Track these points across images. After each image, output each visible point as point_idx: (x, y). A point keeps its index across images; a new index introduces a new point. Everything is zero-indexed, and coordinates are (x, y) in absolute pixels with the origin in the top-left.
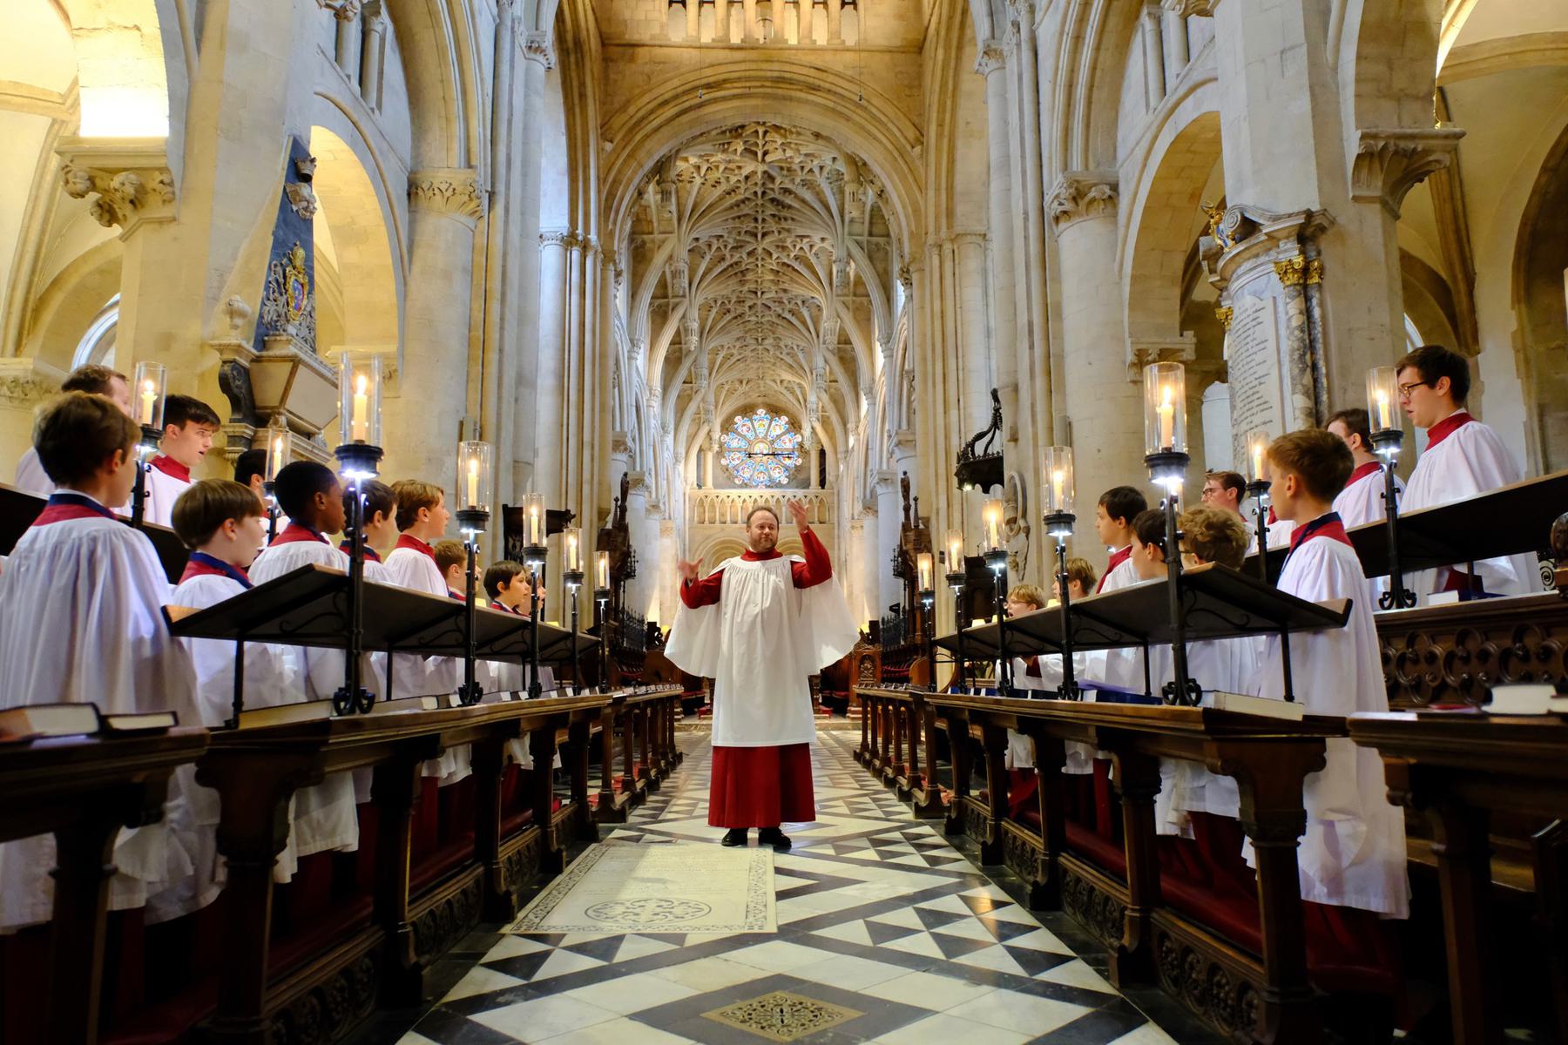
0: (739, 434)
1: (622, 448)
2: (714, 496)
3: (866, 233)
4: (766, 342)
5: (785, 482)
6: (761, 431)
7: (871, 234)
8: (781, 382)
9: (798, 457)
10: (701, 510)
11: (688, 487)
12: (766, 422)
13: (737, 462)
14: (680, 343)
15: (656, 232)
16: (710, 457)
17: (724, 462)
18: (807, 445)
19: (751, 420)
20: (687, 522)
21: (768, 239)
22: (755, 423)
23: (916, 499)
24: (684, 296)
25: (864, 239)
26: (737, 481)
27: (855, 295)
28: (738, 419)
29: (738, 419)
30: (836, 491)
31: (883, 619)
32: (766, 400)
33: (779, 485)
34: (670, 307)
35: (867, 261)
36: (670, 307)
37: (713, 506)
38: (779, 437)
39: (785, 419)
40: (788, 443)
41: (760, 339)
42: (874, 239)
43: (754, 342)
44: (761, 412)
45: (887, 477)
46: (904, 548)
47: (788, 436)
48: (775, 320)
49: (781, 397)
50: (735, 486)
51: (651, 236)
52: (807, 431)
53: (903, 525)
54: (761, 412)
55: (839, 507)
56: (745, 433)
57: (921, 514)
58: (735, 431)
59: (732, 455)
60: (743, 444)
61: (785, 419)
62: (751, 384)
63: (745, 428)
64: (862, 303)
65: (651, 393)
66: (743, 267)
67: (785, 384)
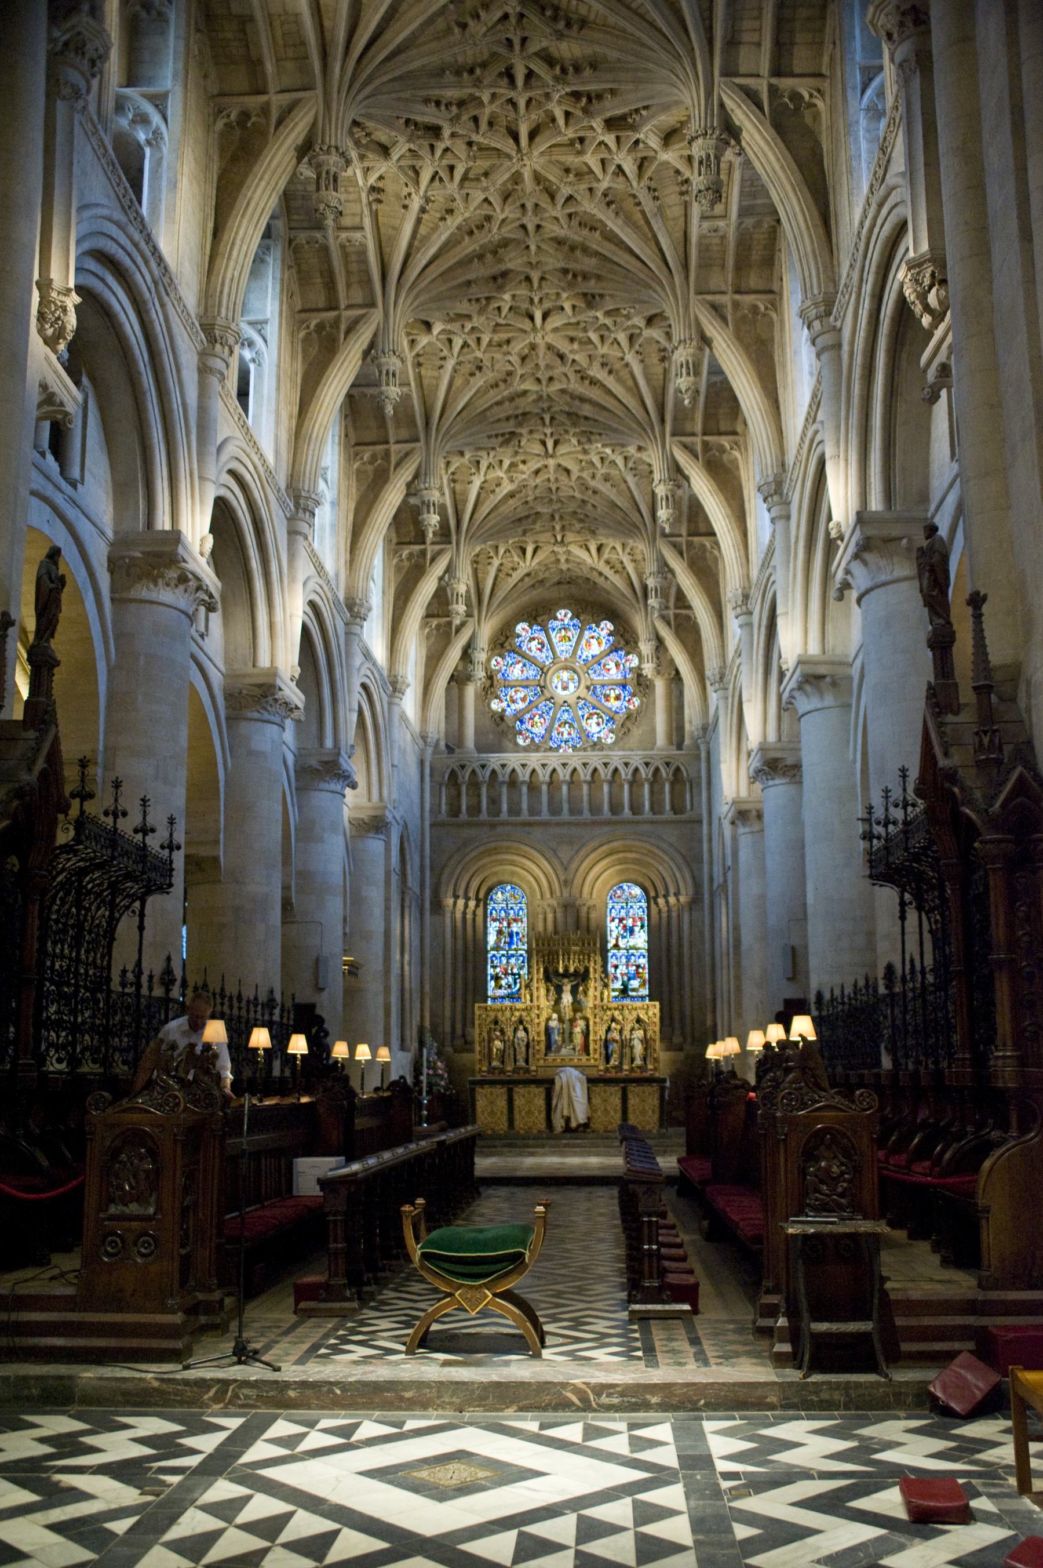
0: (524, 656)
1: (173, 574)
2: (476, 765)
3: (765, 67)
4: (562, 449)
5: (609, 741)
6: (563, 648)
7: (777, 72)
8: (599, 549)
9: (634, 695)
10: (454, 792)
11: (430, 750)
12: (573, 634)
13: (521, 705)
14: (387, 442)
15: (272, 87)
16: (471, 692)
17: (495, 706)
18: (648, 669)
19: (545, 629)
20: (427, 814)
21: (543, 144)
22: (553, 635)
23: (976, 601)
24: (372, 305)
25: (762, 87)
26: (520, 741)
27: (738, 291)
28: (521, 628)
29: (521, 628)
30: (703, 755)
31: (819, 996)
32: (574, 590)
33: (598, 745)
34: (343, 327)
35: (769, 134)
36: (343, 327)
37: (474, 784)
38: (597, 660)
39: (607, 626)
40: (614, 670)
41: (550, 444)
42: (786, 83)
43: (538, 449)
44: (564, 615)
45: (822, 670)
46: (942, 762)
47: (614, 656)
48: (575, 386)
49: (600, 581)
50: (517, 748)
51: (262, 99)
52: (646, 647)
53: (932, 692)
54: (564, 615)
55: (709, 783)
56: (535, 653)
57: (998, 655)
58: (517, 651)
59: (512, 692)
60: (531, 672)
61: (607, 626)
62: (541, 556)
63: (534, 644)
64: (755, 309)
65: (297, 505)
66: (494, 234)
67: (606, 555)
